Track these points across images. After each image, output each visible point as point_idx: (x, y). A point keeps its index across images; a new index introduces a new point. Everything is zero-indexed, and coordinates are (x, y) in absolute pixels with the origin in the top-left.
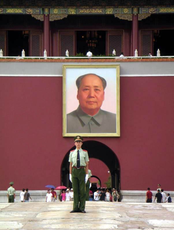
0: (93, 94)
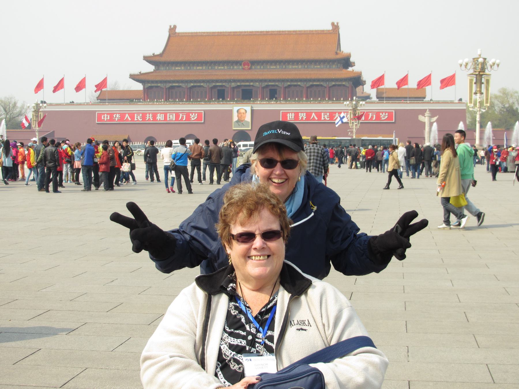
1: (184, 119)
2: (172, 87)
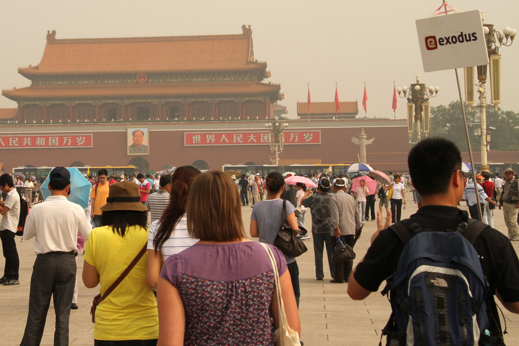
0: (139, 138)
1: (69, 144)
2: (54, 105)
